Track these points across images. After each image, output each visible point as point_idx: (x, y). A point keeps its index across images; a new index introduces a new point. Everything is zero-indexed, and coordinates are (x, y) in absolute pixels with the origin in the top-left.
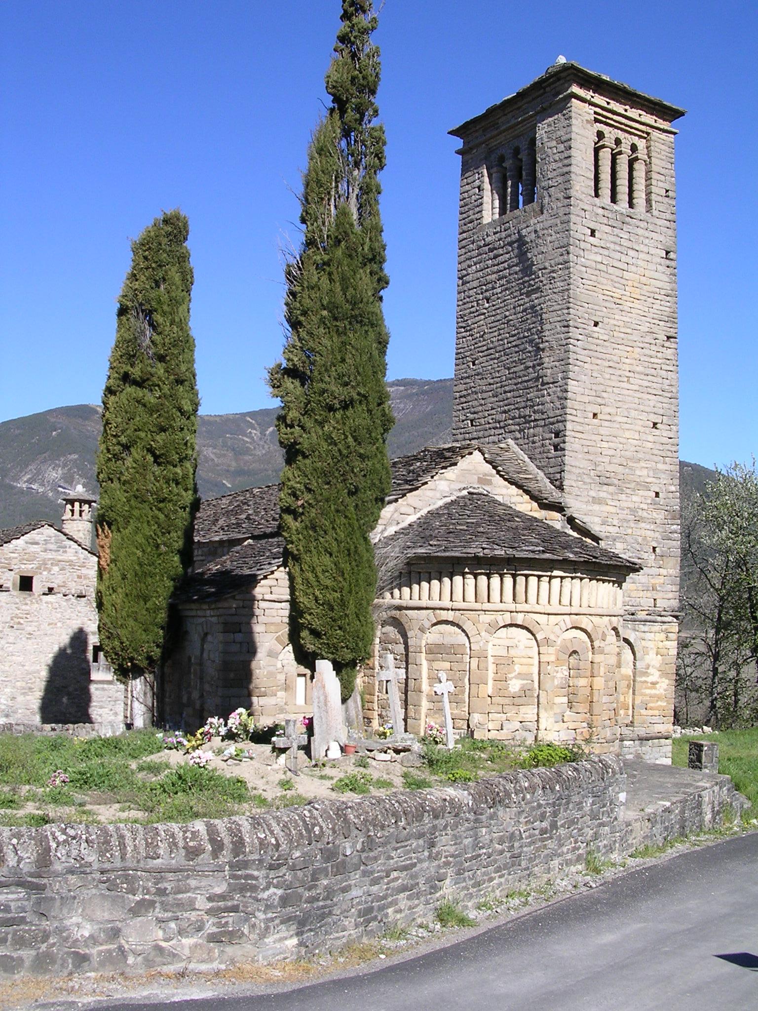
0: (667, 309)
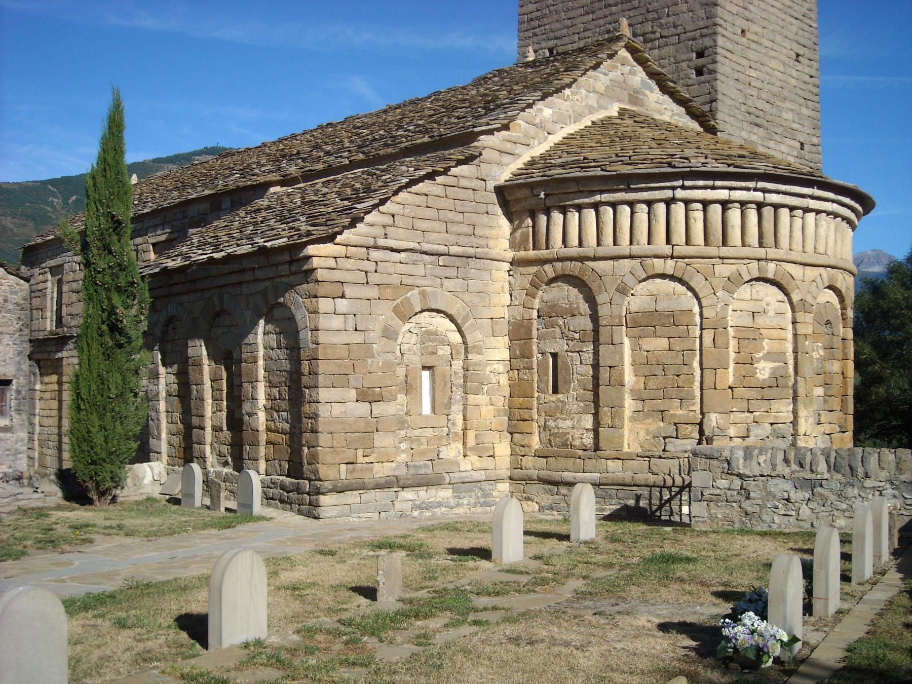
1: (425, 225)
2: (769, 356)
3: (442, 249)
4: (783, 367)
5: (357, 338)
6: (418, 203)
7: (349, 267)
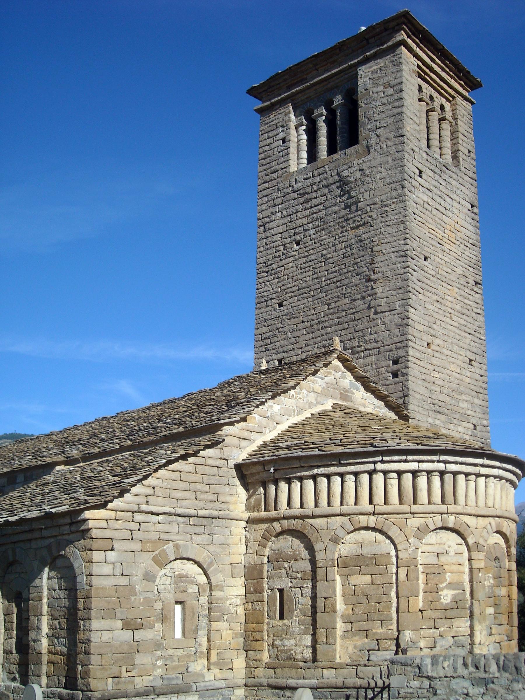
0: (474, 257)
1: (179, 494)
2: (451, 586)
3: (192, 512)
4: (462, 594)
5: (124, 581)
6: (174, 478)
7: (117, 527)
